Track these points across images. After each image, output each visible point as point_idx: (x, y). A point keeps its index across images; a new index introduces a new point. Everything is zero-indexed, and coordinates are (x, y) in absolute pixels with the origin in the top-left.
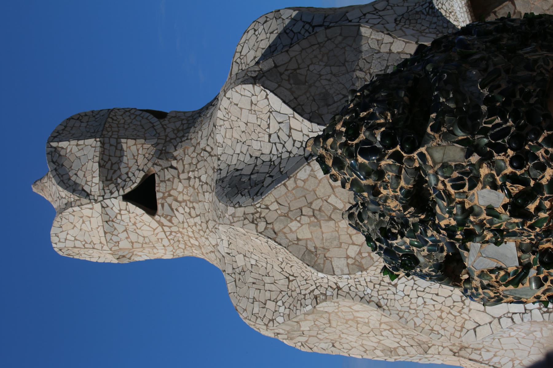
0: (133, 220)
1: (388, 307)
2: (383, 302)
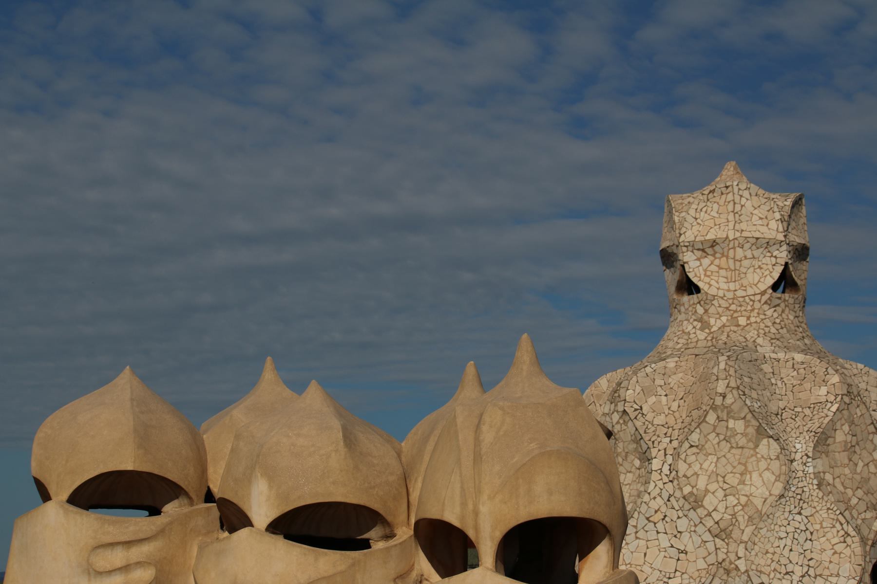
2: (783, 500)
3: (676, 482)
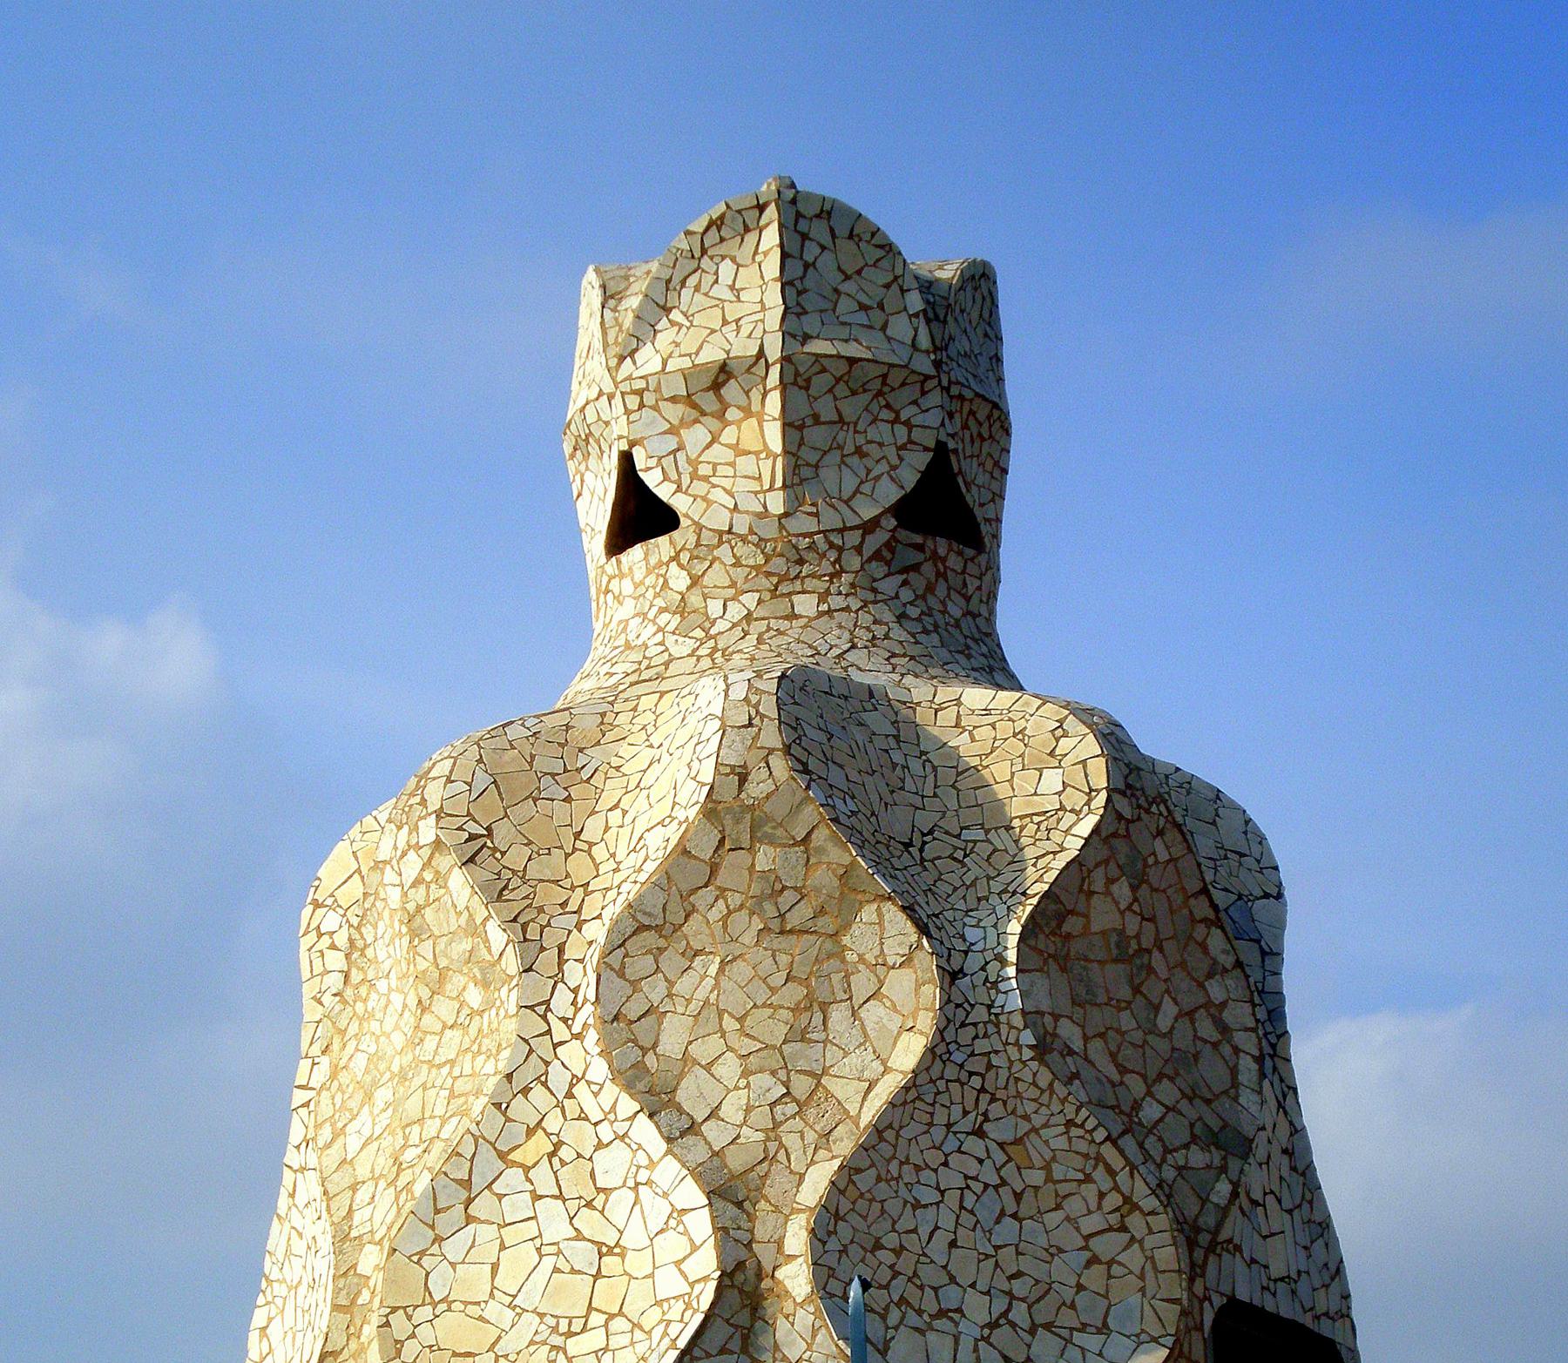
0: (872, 449)
1: (913, 1101)
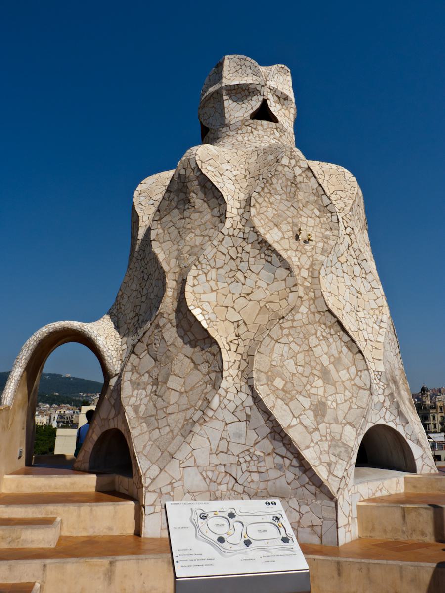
3: (352, 237)
